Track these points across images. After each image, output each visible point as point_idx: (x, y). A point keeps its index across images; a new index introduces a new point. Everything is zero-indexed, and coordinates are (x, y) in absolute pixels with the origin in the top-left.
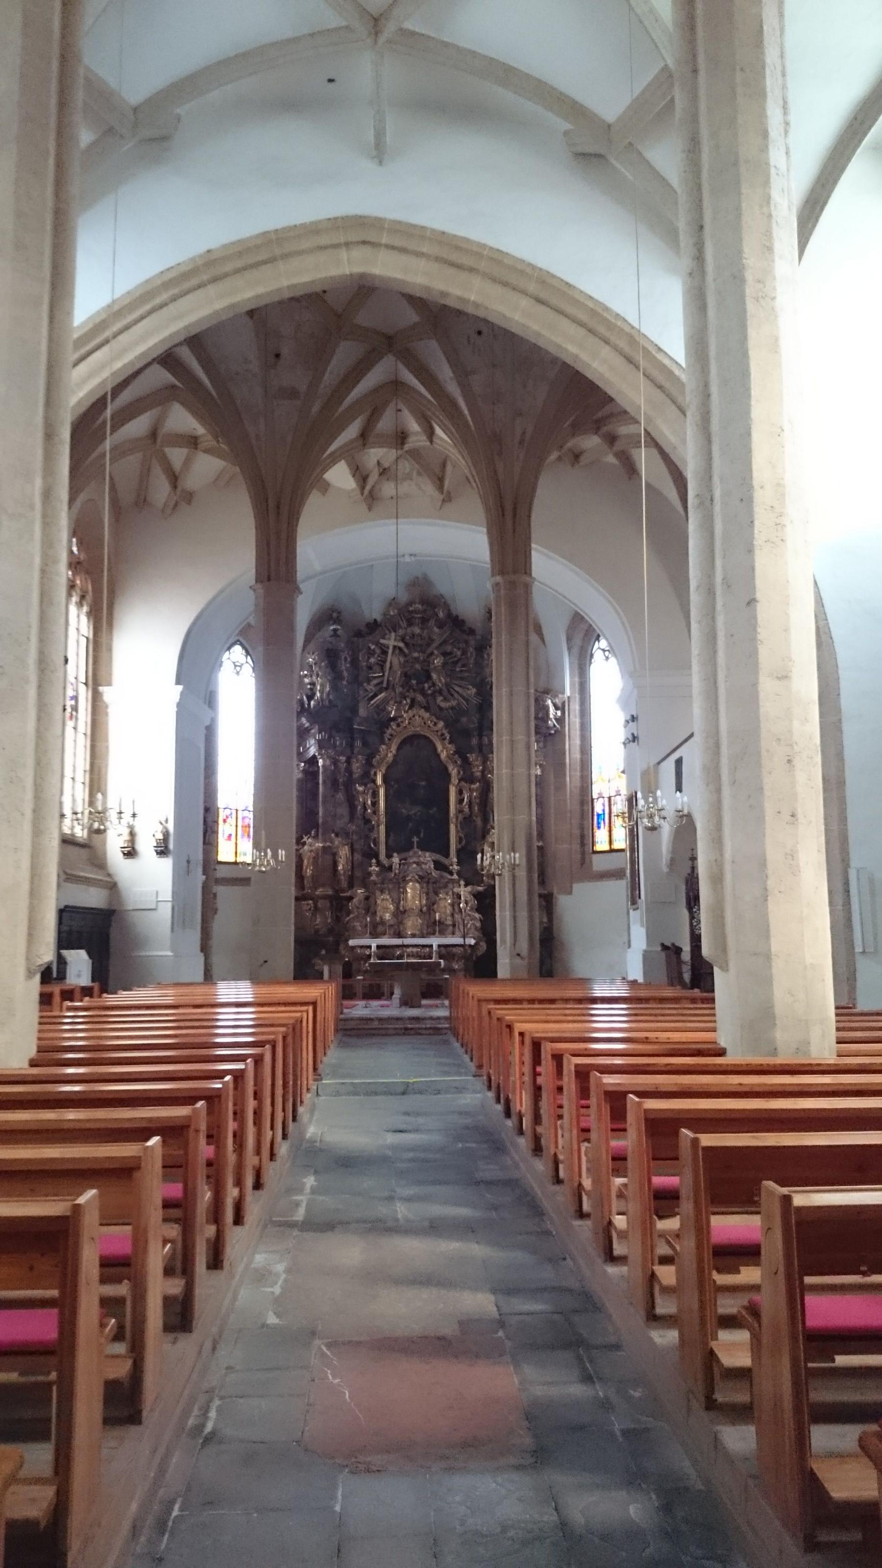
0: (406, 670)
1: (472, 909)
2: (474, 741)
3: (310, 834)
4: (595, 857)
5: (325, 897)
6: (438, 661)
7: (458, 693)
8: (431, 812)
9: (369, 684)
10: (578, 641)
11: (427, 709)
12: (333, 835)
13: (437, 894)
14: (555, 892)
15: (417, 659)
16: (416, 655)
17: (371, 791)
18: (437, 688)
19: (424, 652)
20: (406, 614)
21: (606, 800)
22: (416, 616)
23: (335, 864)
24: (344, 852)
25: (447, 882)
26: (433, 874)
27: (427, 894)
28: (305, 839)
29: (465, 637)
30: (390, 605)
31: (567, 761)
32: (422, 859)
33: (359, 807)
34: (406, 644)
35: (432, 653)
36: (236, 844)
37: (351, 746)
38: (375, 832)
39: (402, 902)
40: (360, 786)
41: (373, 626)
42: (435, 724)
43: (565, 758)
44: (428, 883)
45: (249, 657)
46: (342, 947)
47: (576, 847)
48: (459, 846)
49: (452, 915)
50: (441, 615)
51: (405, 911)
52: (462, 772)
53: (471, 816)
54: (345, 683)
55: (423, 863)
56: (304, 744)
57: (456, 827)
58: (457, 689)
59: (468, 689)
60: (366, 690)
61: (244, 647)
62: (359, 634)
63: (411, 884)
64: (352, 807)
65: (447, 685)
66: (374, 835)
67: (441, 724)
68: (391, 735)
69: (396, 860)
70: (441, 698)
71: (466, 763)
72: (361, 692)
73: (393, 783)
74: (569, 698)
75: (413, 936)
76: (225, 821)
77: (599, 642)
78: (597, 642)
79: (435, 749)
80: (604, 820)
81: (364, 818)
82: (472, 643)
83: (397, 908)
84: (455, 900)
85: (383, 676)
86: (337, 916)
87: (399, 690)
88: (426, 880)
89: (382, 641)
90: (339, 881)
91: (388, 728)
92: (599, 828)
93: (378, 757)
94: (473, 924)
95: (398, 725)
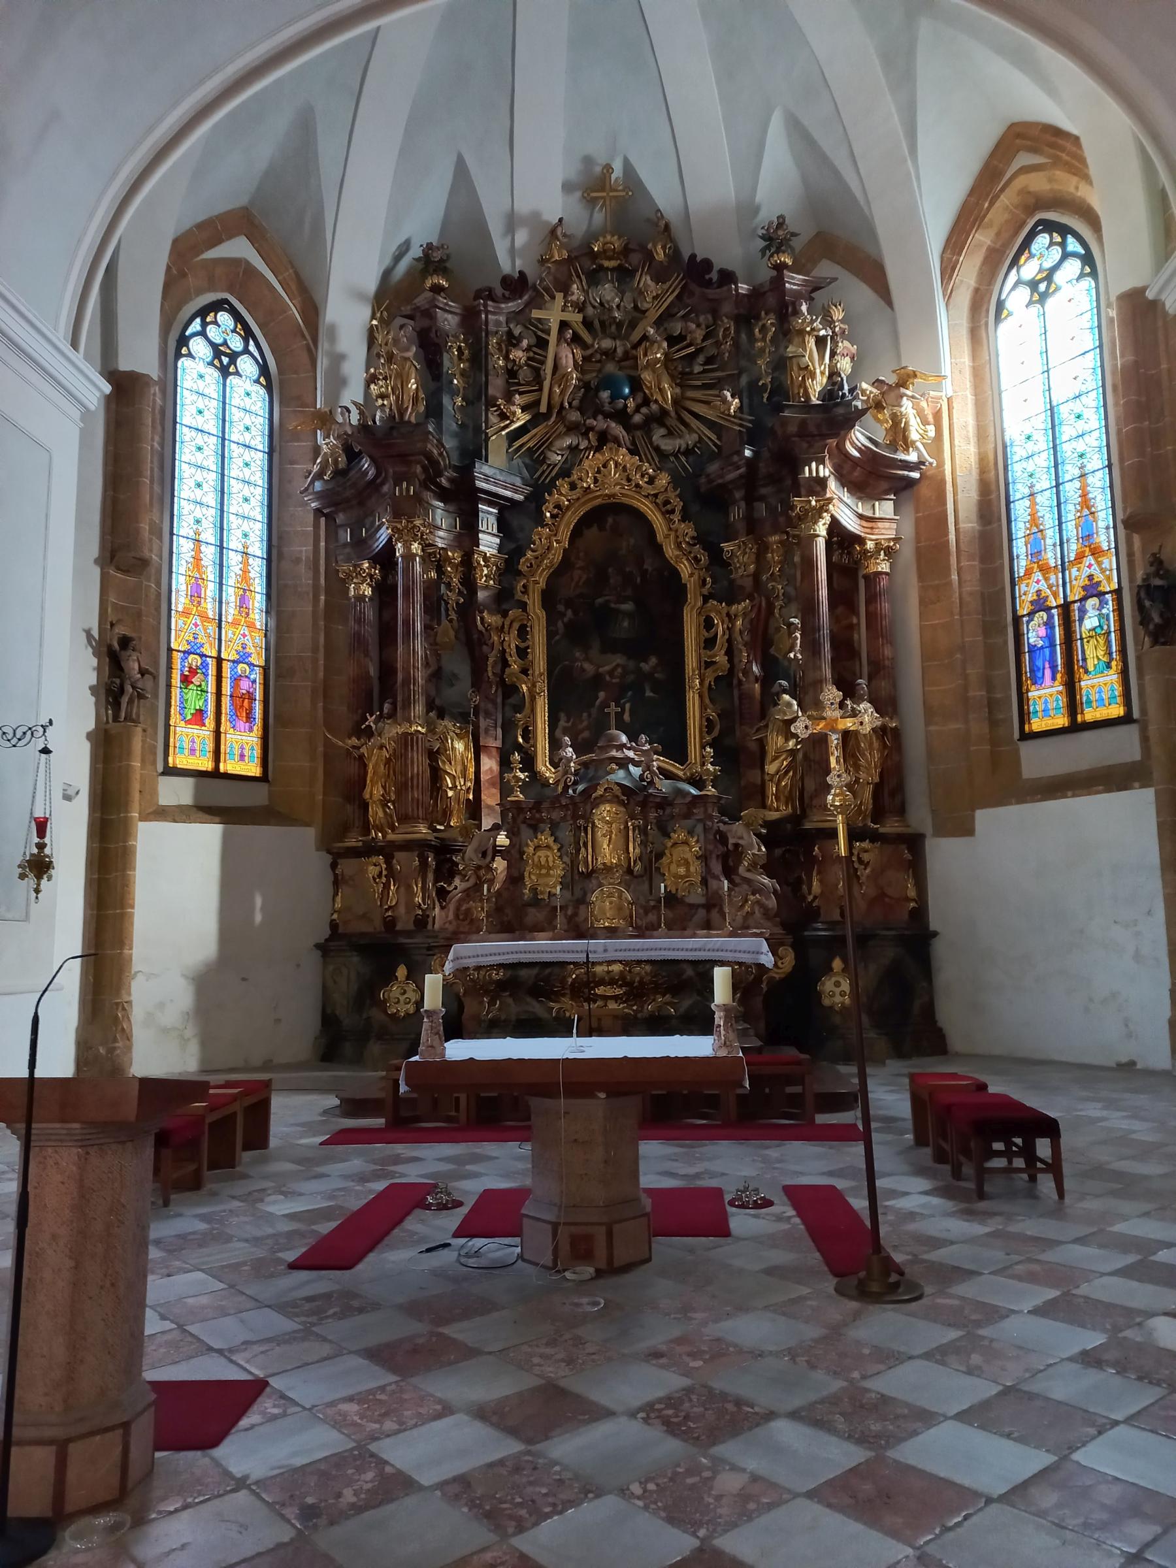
0: (588, 377)
1: (753, 866)
2: (737, 513)
7: (696, 416)
8: (645, 667)
11: (633, 452)
15: (609, 354)
16: (607, 343)
17: (516, 625)
18: (654, 407)
22: (607, 264)
27: (643, 831)
28: (371, 720)
29: (711, 293)
30: (553, 232)
31: (952, 536)
32: (631, 754)
33: (491, 660)
34: (587, 323)
36: (217, 734)
39: (583, 849)
41: (516, 285)
42: (651, 481)
43: (947, 534)
44: (644, 804)
47: (978, 727)
49: (704, 882)
50: (660, 255)
53: (731, 671)
55: (632, 761)
56: (368, 521)
57: (701, 696)
60: (503, 416)
61: (237, 317)
65: (676, 402)
67: (663, 480)
68: (558, 506)
70: (663, 431)
71: (718, 561)
72: (493, 419)
75: (612, 933)
76: (186, 680)
79: (652, 533)
81: (502, 680)
83: (574, 864)
84: (710, 847)
85: (541, 390)
87: (574, 416)
88: (640, 798)
89: (536, 314)
93: (529, 554)
95: (573, 486)
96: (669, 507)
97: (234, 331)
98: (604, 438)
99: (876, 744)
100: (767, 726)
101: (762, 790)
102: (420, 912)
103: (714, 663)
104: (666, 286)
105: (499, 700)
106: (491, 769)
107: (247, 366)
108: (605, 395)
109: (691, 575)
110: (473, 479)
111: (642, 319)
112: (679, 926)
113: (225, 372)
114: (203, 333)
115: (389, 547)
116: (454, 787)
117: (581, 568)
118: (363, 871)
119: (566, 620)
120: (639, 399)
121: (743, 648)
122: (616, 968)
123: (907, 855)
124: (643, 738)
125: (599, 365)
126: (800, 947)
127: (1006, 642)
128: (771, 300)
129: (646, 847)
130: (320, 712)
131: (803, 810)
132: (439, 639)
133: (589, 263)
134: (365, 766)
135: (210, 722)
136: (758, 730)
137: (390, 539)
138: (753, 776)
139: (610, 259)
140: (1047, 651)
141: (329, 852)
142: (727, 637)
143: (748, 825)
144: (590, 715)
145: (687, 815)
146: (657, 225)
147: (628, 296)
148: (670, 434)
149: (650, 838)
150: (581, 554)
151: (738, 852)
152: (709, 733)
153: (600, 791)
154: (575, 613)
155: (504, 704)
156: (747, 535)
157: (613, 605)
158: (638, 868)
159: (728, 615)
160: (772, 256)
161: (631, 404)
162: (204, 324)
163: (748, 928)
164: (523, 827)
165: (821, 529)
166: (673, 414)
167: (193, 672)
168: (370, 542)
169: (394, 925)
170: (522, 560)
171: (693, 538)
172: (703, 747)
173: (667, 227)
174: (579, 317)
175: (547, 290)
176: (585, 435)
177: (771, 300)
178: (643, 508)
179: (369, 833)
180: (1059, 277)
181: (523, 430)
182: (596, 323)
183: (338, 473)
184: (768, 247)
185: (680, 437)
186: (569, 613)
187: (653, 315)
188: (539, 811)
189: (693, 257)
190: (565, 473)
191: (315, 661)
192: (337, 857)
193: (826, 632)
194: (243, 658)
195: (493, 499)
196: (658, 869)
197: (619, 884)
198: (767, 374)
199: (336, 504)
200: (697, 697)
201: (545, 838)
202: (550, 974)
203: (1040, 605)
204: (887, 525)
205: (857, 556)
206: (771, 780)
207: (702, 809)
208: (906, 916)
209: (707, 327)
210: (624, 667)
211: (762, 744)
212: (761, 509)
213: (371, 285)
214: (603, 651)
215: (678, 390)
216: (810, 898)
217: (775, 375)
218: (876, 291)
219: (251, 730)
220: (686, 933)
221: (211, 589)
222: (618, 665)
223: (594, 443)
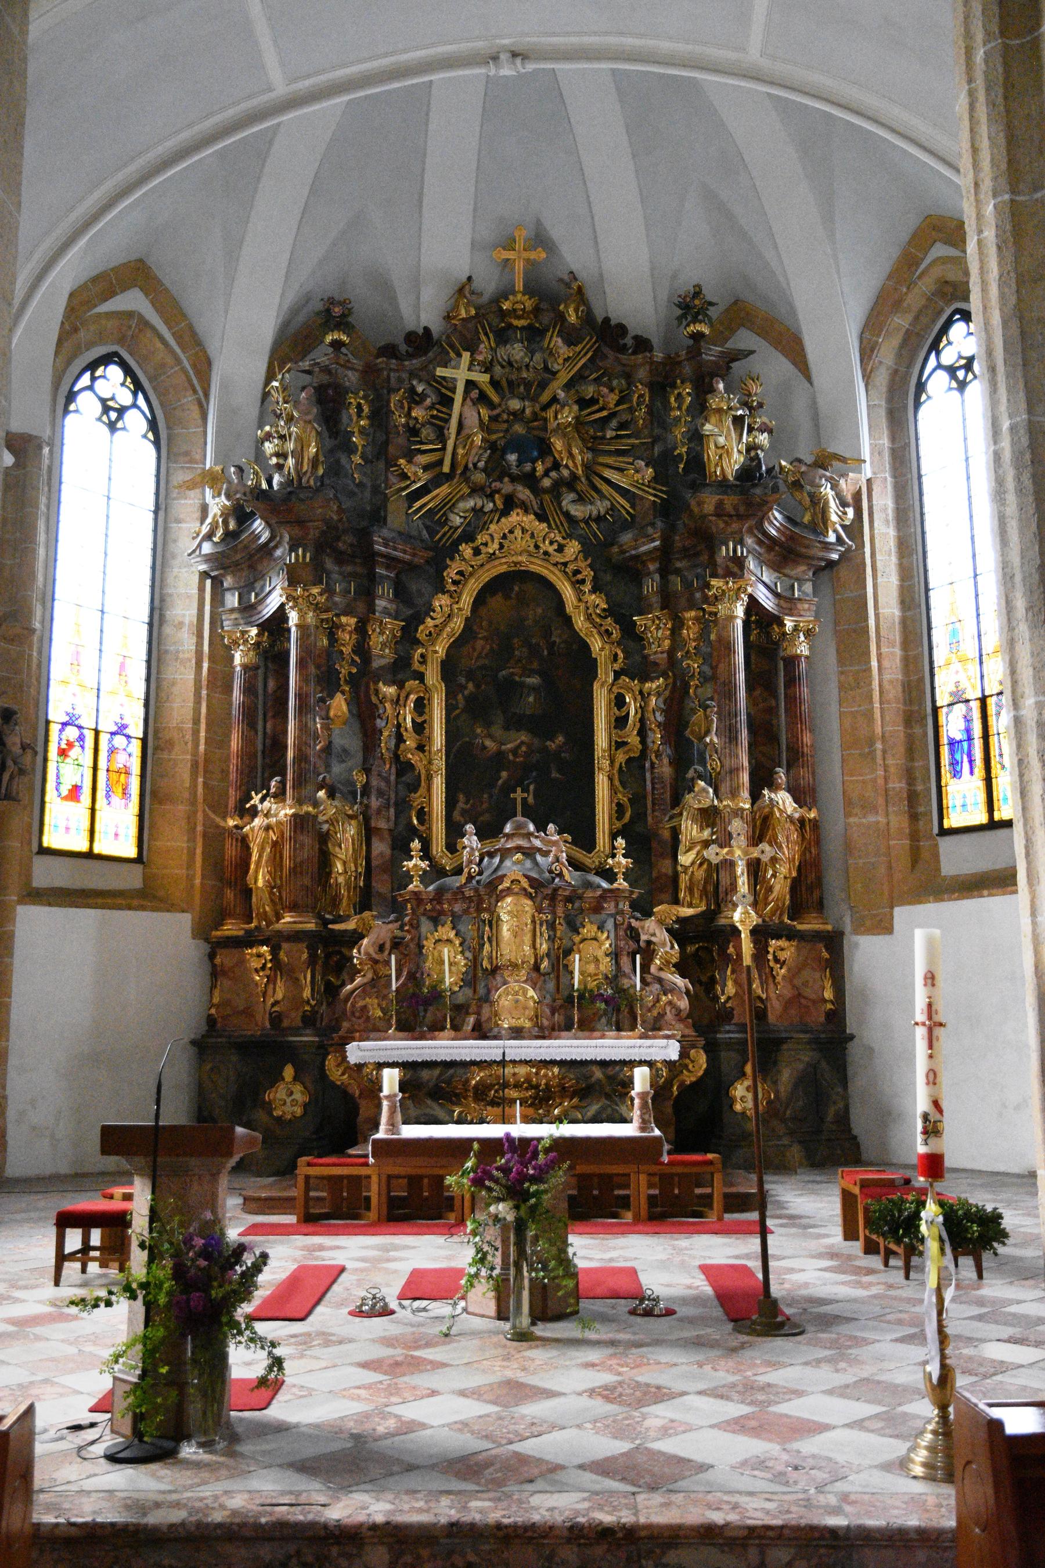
0: (494, 437)
2: (651, 586)
3: (268, 790)
4: (946, 844)
5: (295, 936)
6: (567, 416)
7: (608, 481)
8: (552, 745)
9: (410, 461)
10: (887, 353)
11: (542, 517)
12: (321, 794)
13: (574, 927)
14: (848, 928)
16: (515, 404)
17: (413, 697)
19: (534, 399)
20: (495, 321)
21: (975, 706)
22: (516, 323)
23: (325, 860)
24: (349, 833)
25: (601, 896)
26: (567, 877)
27: (552, 926)
28: (256, 799)
31: (872, 622)
32: (537, 843)
33: (386, 734)
34: (494, 383)
35: (554, 400)
36: (93, 810)
37: (367, 594)
38: (422, 790)
39: (487, 946)
42: (560, 549)
44: (553, 898)
45: (140, 396)
46: (331, 1061)
47: (898, 821)
48: (618, 825)
50: (572, 318)
51: (495, 970)
52: (621, 655)
54: (357, 459)
55: (539, 850)
56: (258, 585)
59: (637, 471)
60: (404, 476)
61: (128, 371)
62: (389, 351)
63: (509, 900)
64: (370, 737)
65: (587, 467)
66: (417, 799)
67: (573, 548)
69: (471, 841)
70: (572, 496)
71: (631, 637)
72: (393, 479)
73: (463, 680)
74: (869, 481)
75: (517, 1033)
76: (63, 753)
77: (938, 354)
78: (933, 355)
81: (396, 757)
82: (642, 373)
83: (475, 963)
85: (444, 449)
86: (328, 985)
87: (479, 477)
89: (440, 372)
90: (335, 901)
91: (452, 559)
92: (956, 774)
94: (670, 1003)
95: (477, 552)
96: (580, 577)
97: (123, 384)
98: (510, 504)
99: (795, 836)
100: (681, 814)
101: (675, 879)
102: (307, 1008)
103: (625, 743)
104: (578, 349)
105: (393, 778)
106: (381, 854)
107: (136, 422)
108: (512, 458)
109: (602, 649)
110: (371, 543)
111: (550, 381)
112: (587, 1027)
113: (112, 426)
115: (281, 614)
116: (345, 872)
117: (485, 638)
118: (242, 962)
119: (466, 692)
120: (549, 463)
121: (657, 730)
122: (522, 1071)
123: (826, 955)
124: (551, 827)
125: (505, 426)
126: (711, 1049)
127: (925, 734)
128: (687, 370)
129: (553, 941)
131: (718, 905)
132: (332, 714)
133: (497, 320)
134: (248, 848)
136: (672, 818)
137: (282, 605)
138: (665, 866)
139: (519, 318)
140: (965, 744)
141: (207, 940)
142: (639, 716)
143: (660, 922)
144: (491, 796)
146: (568, 285)
147: (538, 357)
148: (581, 499)
149: (558, 934)
150: (484, 623)
151: (648, 951)
152: (619, 819)
153: (506, 884)
154: (477, 686)
155: (397, 783)
156: (662, 609)
157: (517, 678)
158: (545, 964)
159: (641, 692)
160: (688, 325)
161: (540, 468)
163: (660, 1029)
164: (423, 919)
165: (740, 611)
166: (583, 479)
167: (70, 745)
168: (260, 608)
169: (281, 1021)
170: (421, 628)
171: (604, 610)
172: (613, 837)
173: (580, 288)
174: (485, 378)
175: (452, 346)
176: (491, 497)
177: (687, 370)
178: (552, 578)
181: (424, 491)
182: (504, 383)
183: (228, 535)
184: (684, 316)
185: (592, 503)
186: (470, 685)
187: (564, 377)
188: (440, 903)
189: (607, 320)
190: (468, 537)
191: (196, 733)
192: (216, 947)
193: (744, 717)
194: (121, 730)
195: (391, 562)
196: (566, 966)
197: (525, 982)
198: (683, 444)
199: (224, 568)
200: (606, 779)
201: (446, 932)
202: (452, 1076)
203: (960, 698)
204: (806, 606)
205: (775, 637)
206: (685, 873)
207: (613, 904)
208: (822, 1019)
209: (621, 392)
210: (529, 746)
211: (675, 832)
212: (676, 583)
214: (507, 728)
215: (589, 455)
217: (692, 445)
218: (795, 364)
219: (126, 805)
220: (597, 1034)
222: (522, 743)
223: (500, 504)
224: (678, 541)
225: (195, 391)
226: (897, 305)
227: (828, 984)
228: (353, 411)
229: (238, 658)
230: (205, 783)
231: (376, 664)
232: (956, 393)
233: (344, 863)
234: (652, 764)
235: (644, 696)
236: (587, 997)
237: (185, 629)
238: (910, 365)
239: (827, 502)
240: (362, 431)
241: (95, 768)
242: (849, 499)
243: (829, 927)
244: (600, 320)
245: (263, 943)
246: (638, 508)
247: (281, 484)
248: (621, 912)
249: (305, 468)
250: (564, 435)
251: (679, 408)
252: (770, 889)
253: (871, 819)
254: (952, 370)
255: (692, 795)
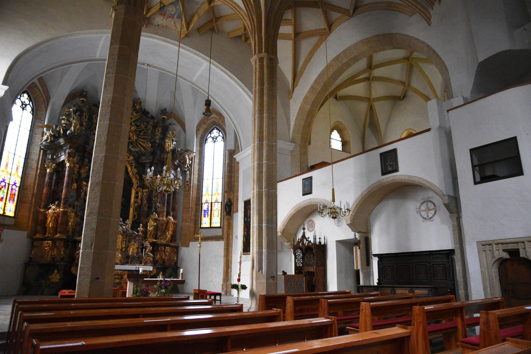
1: (149, 251)
3: (55, 204)
4: (200, 230)
5: (61, 239)
7: (140, 144)
10: (201, 132)
21: (210, 204)
23: (68, 221)
26: (130, 231)
27: (126, 242)
28: (51, 206)
36: (5, 204)
40: (85, 182)
42: (129, 158)
44: (126, 236)
45: (31, 102)
47: (192, 225)
48: (134, 219)
52: (139, 183)
53: (141, 204)
57: (133, 209)
58: (142, 144)
61: (29, 96)
65: (136, 140)
67: (131, 158)
70: (131, 146)
74: (194, 156)
78: (210, 134)
80: (208, 213)
82: (151, 123)
92: (205, 217)
94: (149, 259)
97: (27, 99)
100: (149, 219)
102: (62, 256)
103: (137, 202)
107: (29, 108)
109: (135, 181)
112: (132, 263)
113: (23, 109)
114: (20, 99)
122: (119, 272)
123: (176, 251)
127: (199, 208)
130: (34, 201)
135: (4, 201)
145: (135, 238)
148: (133, 147)
159: (142, 191)
160: (163, 116)
162: (21, 96)
171: (136, 172)
173: (140, 102)
179: (45, 234)
180: (218, 139)
184: (162, 113)
189: (145, 110)
191: (34, 187)
194: (15, 184)
197: (119, 253)
203: (207, 202)
208: (174, 264)
213: (66, 96)
215: (137, 138)
216: (157, 259)
219: (13, 203)
221: (10, 166)
224: (155, 161)
225: (45, 104)
226: (205, 123)
227: (176, 257)
228: (84, 117)
229: (48, 170)
230: (35, 200)
231: (82, 177)
232: (213, 143)
233: (72, 223)
234: (143, 208)
235: (143, 193)
236: (133, 258)
237: (34, 161)
238: (205, 134)
239: (186, 159)
240: (86, 122)
241: (7, 193)
242: (190, 159)
243: (177, 245)
244: (143, 109)
245: (49, 240)
246: (146, 151)
247: (69, 133)
248: (140, 239)
249: (76, 131)
250: (132, 133)
251: (158, 132)
252: (167, 237)
253: (188, 224)
254: (213, 138)
255: (152, 215)
